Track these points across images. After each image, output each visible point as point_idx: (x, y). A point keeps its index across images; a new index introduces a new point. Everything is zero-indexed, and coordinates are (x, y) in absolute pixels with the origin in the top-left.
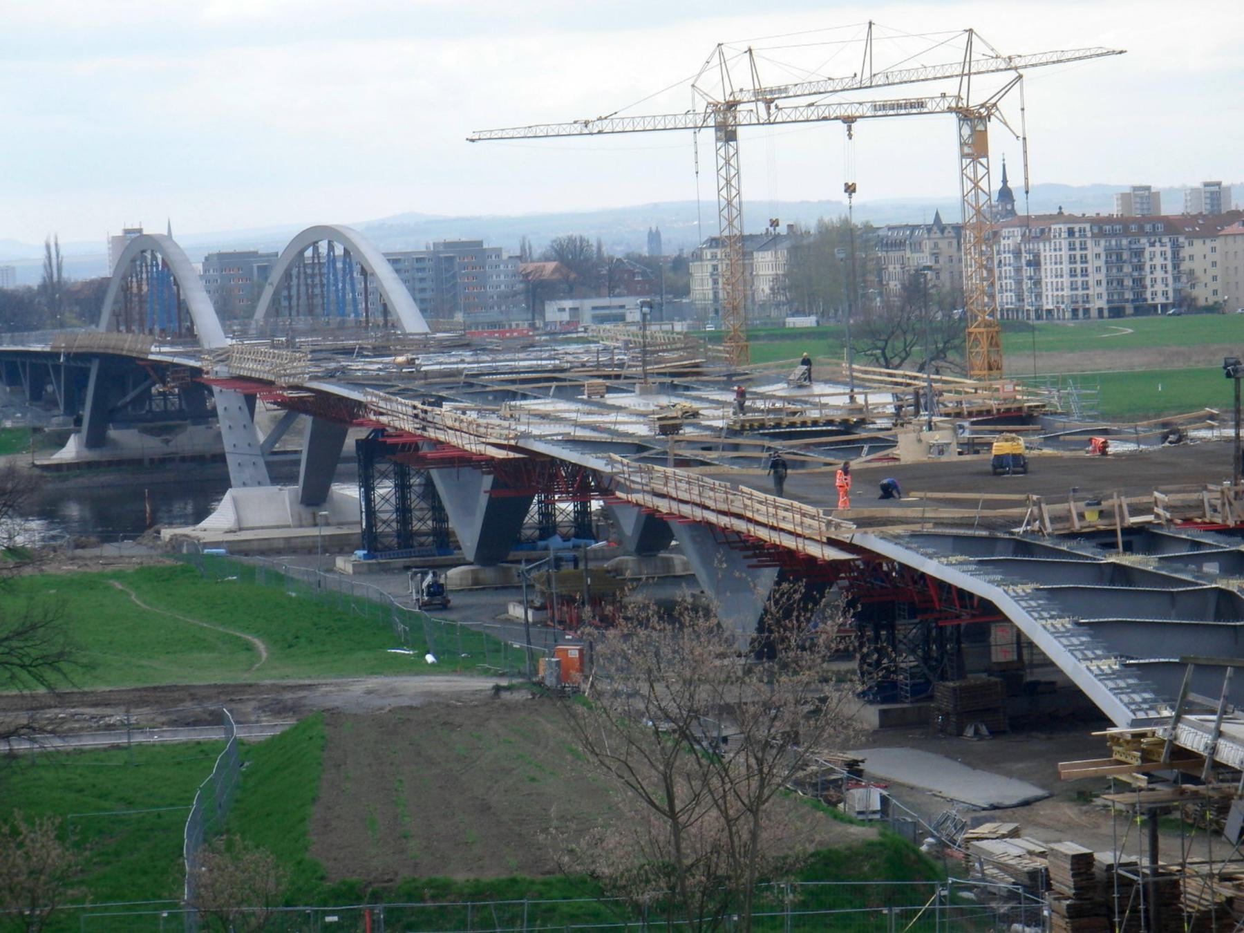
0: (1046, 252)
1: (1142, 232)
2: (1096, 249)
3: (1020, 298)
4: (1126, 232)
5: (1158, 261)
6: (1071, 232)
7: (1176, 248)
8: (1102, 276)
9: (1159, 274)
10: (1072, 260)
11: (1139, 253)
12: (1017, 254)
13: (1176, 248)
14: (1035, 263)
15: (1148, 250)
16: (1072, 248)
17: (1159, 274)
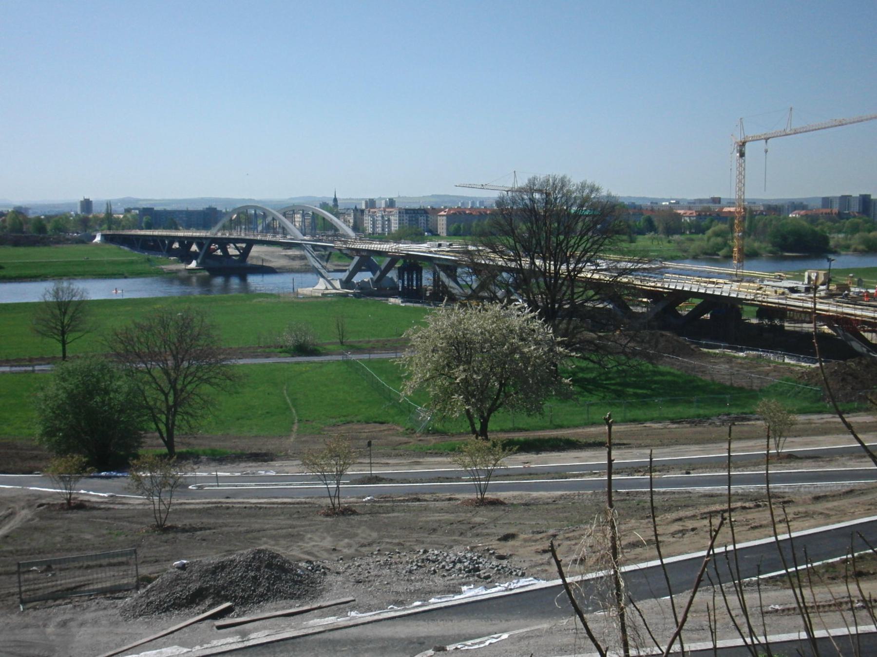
0: (392, 218)
1: (418, 213)
2: (406, 217)
3: (383, 230)
4: (414, 213)
5: (422, 221)
6: (400, 213)
7: (427, 217)
8: (407, 224)
9: (422, 225)
10: (400, 220)
11: (417, 219)
12: (383, 217)
13: (427, 217)
14: (389, 220)
15: (420, 218)
16: (399, 217)
17: (422, 225)
